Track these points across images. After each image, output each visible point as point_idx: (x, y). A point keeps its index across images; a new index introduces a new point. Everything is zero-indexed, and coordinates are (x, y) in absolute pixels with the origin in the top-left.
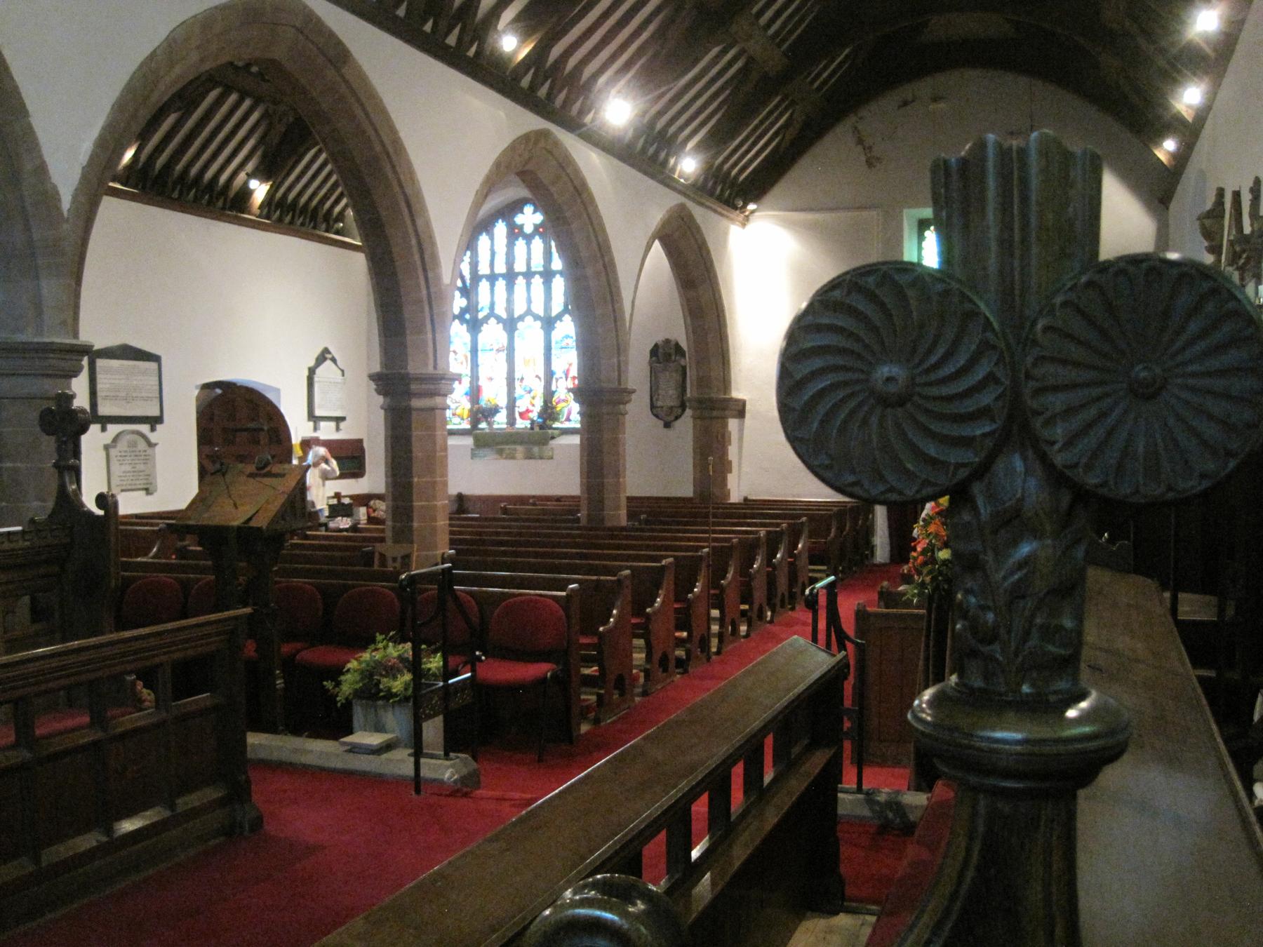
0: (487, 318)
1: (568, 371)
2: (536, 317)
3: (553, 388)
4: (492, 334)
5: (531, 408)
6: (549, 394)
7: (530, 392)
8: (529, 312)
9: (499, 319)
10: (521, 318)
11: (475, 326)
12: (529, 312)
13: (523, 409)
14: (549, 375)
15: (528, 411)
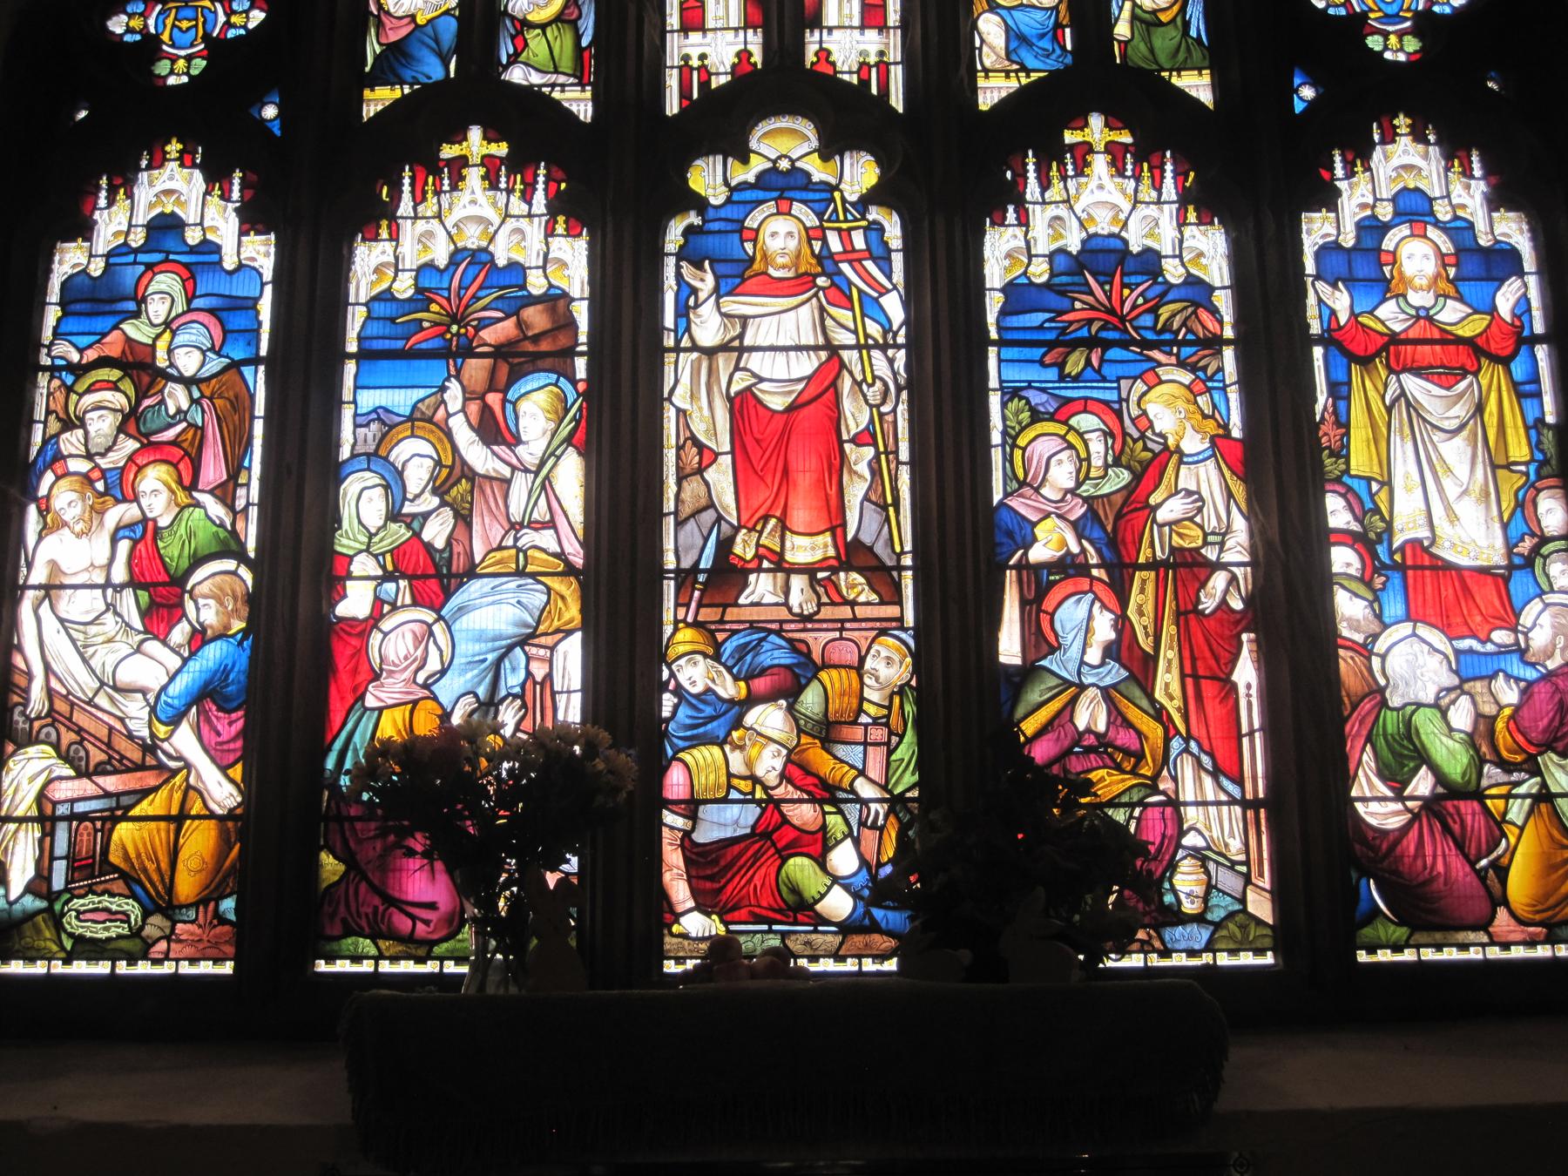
0: (417, 140)
1: (1133, 509)
2: (844, 114)
3: (1010, 649)
4: (480, 220)
5: (804, 814)
6: (963, 699)
7: (790, 691)
8: (785, 79)
9: (531, 131)
10: (724, 117)
11: (321, 186)
12: (785, 79)
13: (726, 822)
14: (962, 551)
15: (774, 837)
